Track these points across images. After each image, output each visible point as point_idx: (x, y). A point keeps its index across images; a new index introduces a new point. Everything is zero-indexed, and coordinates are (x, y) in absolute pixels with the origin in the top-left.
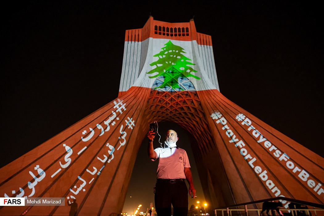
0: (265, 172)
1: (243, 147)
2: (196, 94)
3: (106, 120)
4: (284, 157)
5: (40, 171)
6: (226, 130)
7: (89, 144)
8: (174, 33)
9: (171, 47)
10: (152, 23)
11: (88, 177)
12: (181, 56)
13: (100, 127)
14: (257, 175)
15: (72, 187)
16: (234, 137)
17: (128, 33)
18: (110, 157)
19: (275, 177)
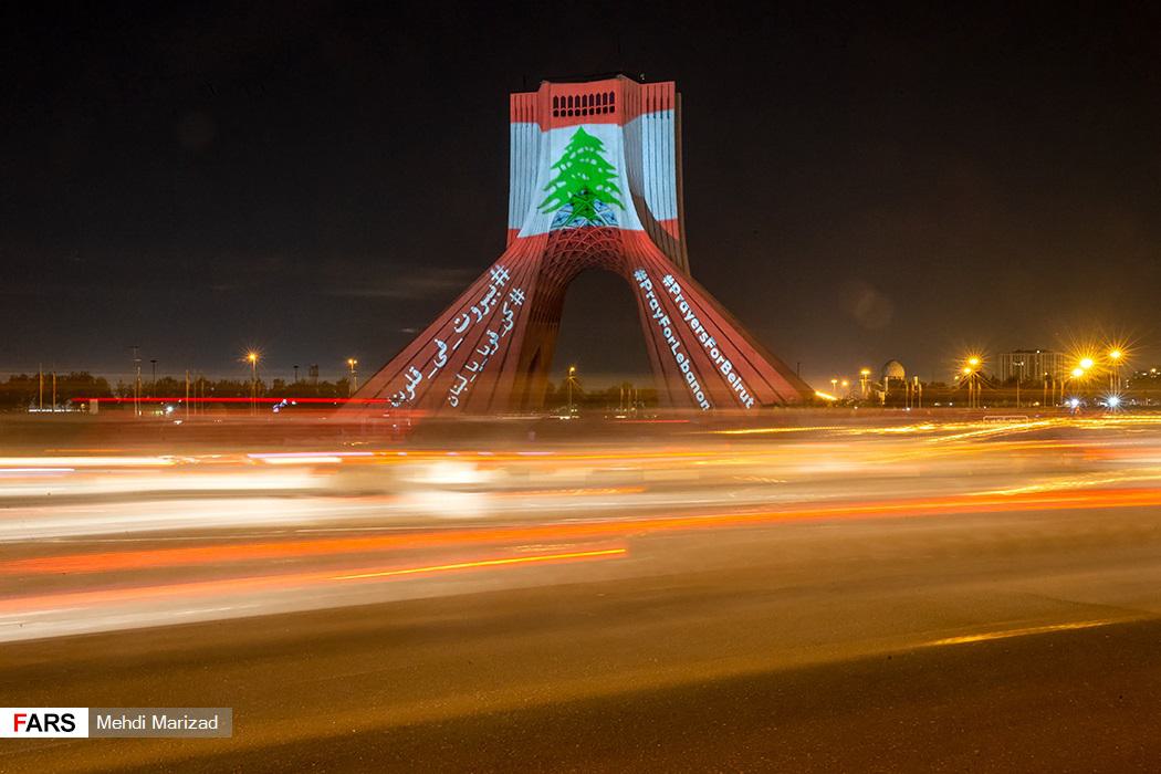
0: (688, 361)
1: (668, 326)
2: (617, 231)
3: (482, 300)
4: (709, 343)
5: (416, 373)
6: (651, 298)
7: (465, 335)
8: (588, 109)
9: (581, 139)
10: (552, 90)
11: (468, 374)
12: (599, 159)
13: (475, 310)
14: (678, 365)
15: (452, 388)
16: (659, 310)
17: (517, 100)
18: (492, 347)
19: (696, 367)
